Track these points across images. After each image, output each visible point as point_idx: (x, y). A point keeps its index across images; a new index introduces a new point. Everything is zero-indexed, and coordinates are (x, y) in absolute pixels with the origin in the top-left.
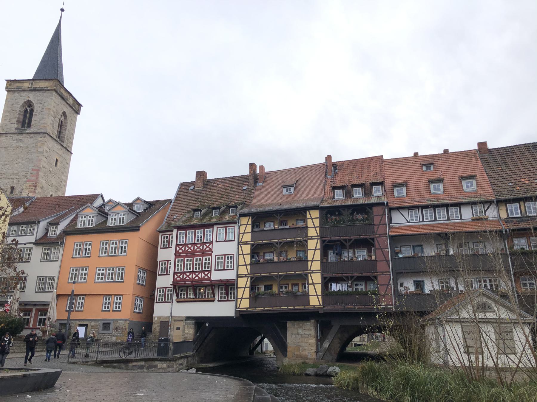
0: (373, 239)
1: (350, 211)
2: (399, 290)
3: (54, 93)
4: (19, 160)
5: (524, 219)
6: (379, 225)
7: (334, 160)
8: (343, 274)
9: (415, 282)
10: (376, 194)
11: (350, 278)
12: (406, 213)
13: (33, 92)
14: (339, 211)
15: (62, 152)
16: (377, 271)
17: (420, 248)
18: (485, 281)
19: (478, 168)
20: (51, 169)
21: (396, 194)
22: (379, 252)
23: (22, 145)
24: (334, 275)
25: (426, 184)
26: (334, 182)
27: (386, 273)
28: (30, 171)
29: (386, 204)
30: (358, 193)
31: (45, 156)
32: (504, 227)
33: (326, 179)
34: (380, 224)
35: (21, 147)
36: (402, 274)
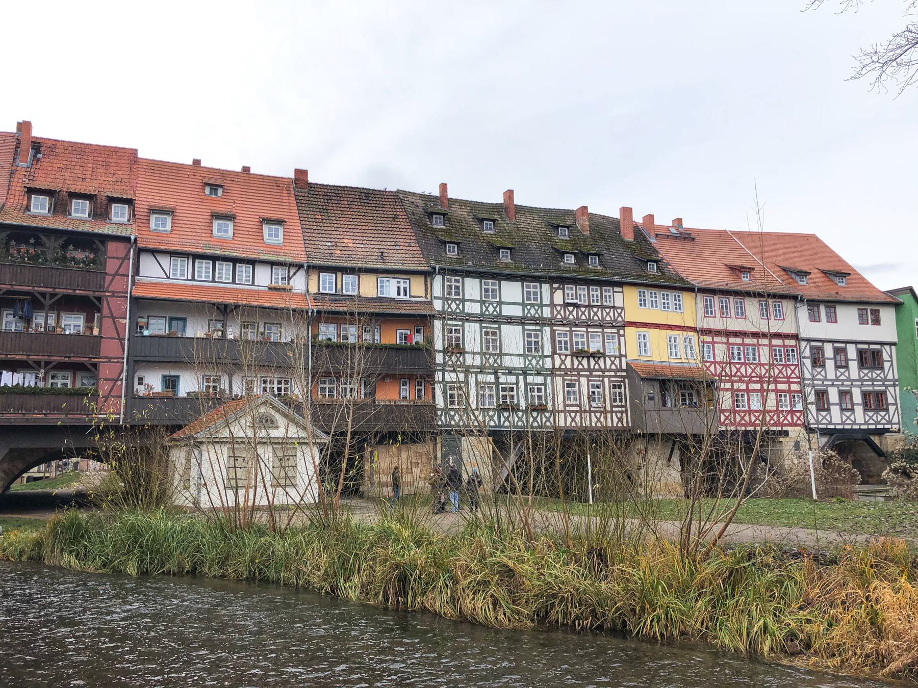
0: (99, 299)
1: (61, 242)
2: (135, 390)
5: (337, 297)
6: (114, 276)
7: (37, 132)
8: (31, 357)
9: (164, 377)
10: (117, 219)
11: (43, 364)
12: (165, 261)
14: (37, 238)
16: (99, 355)
17: (181, 323)
18: (272, 382)
19: (288, 209)
21: (152, 225)
22: (108, 322)
24: (9, 356)
25: (206, 217)
26: (31, 178)
27: (116, 361)
29: (132, 240)
30: (80, 211)
32: (311, 306)
33: (14, 168)
34: (116, 274)
36: (144, 363)
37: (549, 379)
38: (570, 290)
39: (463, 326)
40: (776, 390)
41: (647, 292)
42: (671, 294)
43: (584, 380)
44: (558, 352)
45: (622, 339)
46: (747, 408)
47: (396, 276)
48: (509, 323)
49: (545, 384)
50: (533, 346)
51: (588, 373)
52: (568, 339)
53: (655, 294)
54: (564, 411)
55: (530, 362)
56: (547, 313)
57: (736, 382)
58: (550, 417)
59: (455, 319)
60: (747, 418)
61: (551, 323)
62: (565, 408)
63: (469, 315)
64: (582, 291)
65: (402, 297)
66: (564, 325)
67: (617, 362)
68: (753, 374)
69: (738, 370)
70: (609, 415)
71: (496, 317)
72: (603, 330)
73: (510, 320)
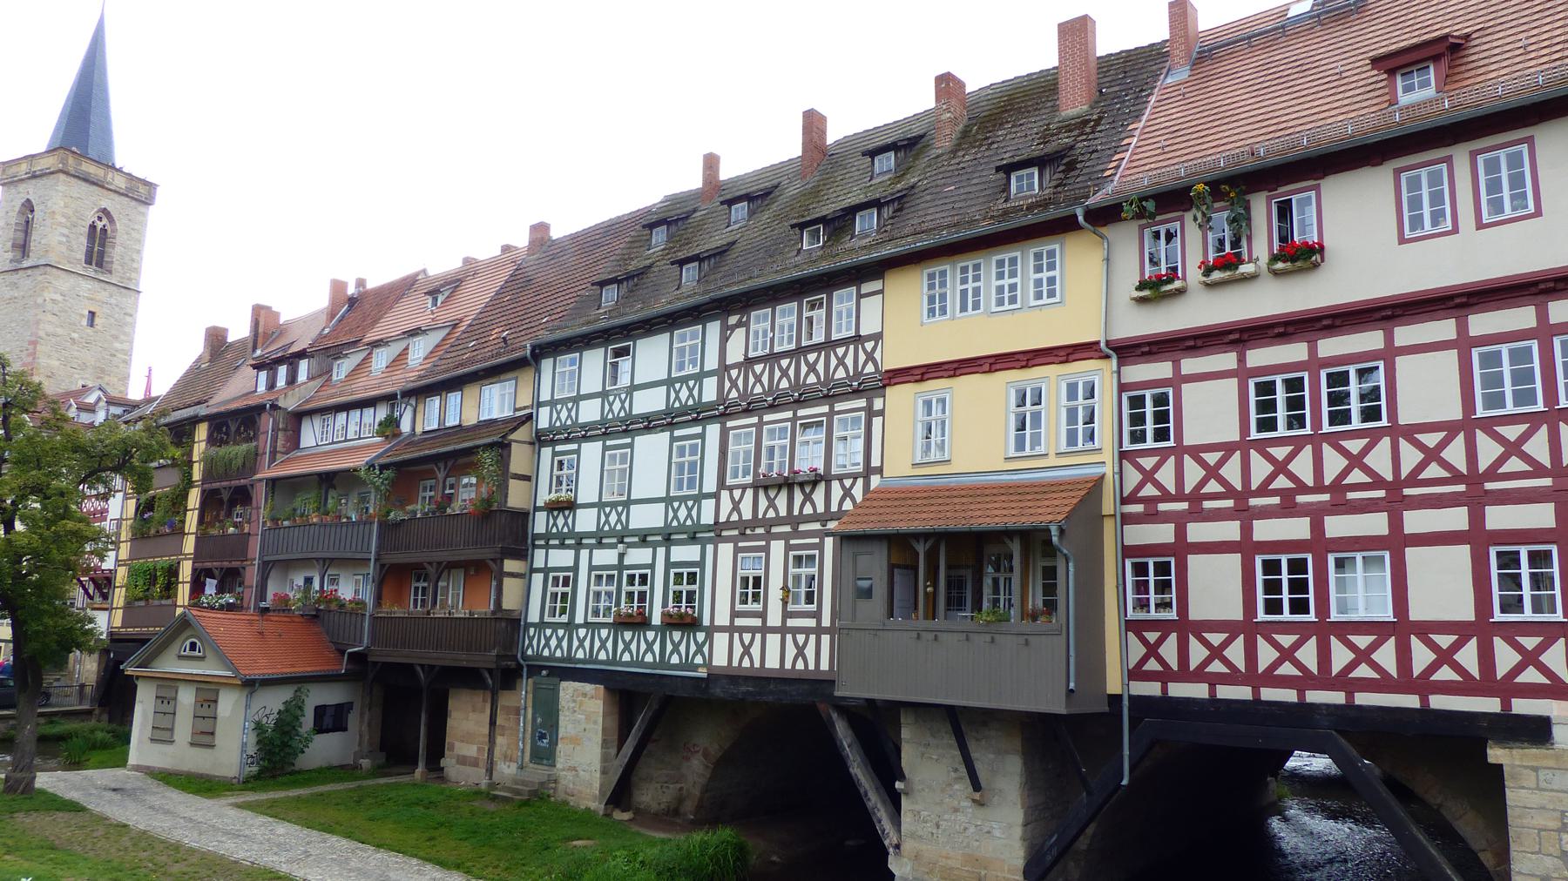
3: (62, 177)
4: (13, 325)
5: (444, 433)
13: (33, 181)
15: (107, 294)
20: (75, 335)
23: (16, 295)
28: (26, 345)
31: (50, 311)
35: (15, 298)
37: (710, 548)
38: (760, 319)
39: (578, 452)
40: (1477, 537)
41: (950, 270)
42: (1024, 256)
43: (777, 547)
44: (729, 481)
45: (877, 421)
46: (1312, 617)
47: (502, 377)
48: (648, 429)
49: (701, 564)
50: (685, 471)
51: (787, 529)
52: (752, 446)
53: (977, 267)
54: (731, 629)
55: (675, 511)
56: (710, 392)
57: (1266, 513)
58: (704, 643)
59: (567, 441)
60: (1308, 655)
61: (722, 412)
62: (732, 621)
63: (583, 426)
64: (787, 314)
65: (508, 413)
66: (747, 412)
67: (858, 492)
68: (1357, 476)
69: (1281, 468)
70: (826, 639)
71: (623, 421)
72: (832, 407)
73: (649, 423)
